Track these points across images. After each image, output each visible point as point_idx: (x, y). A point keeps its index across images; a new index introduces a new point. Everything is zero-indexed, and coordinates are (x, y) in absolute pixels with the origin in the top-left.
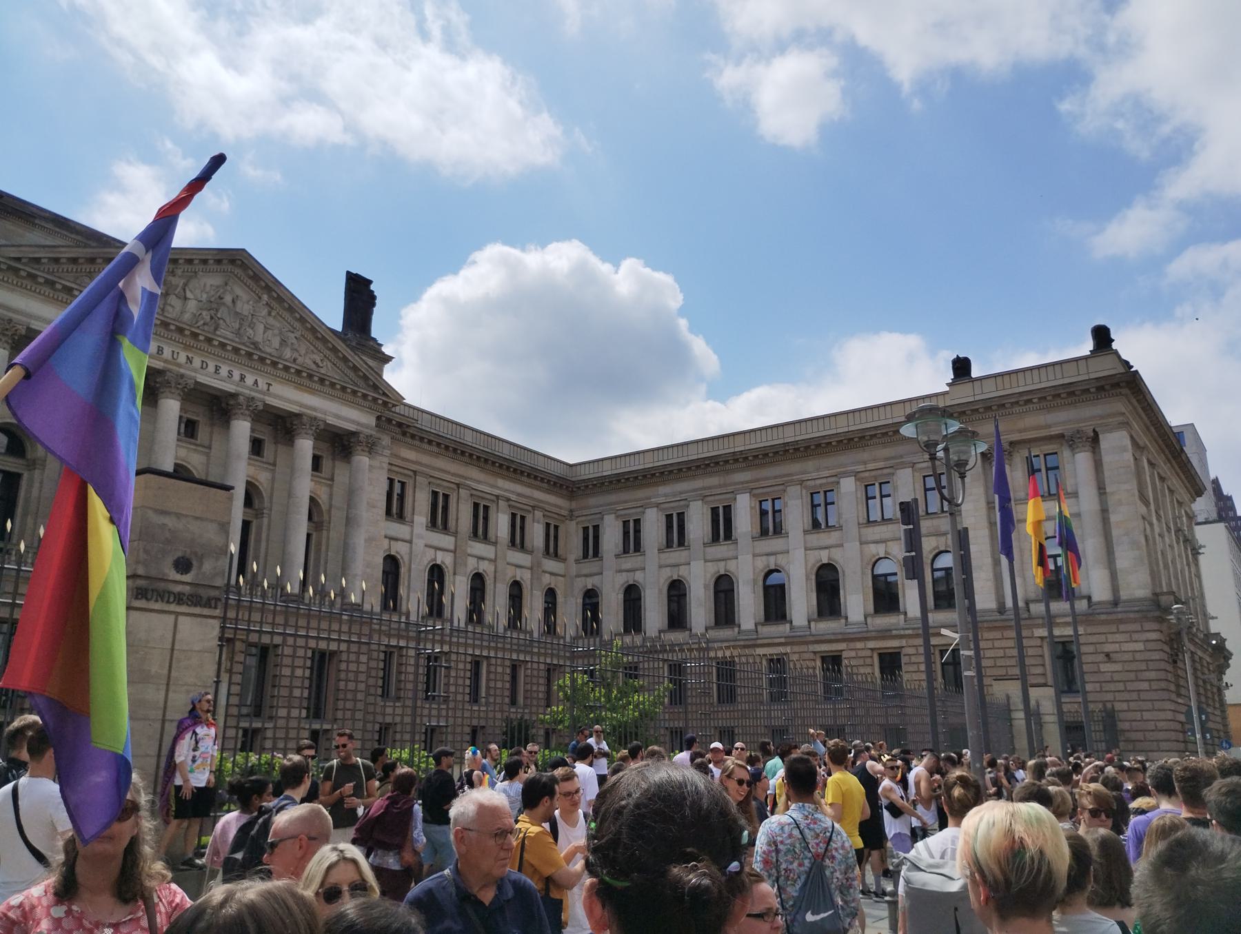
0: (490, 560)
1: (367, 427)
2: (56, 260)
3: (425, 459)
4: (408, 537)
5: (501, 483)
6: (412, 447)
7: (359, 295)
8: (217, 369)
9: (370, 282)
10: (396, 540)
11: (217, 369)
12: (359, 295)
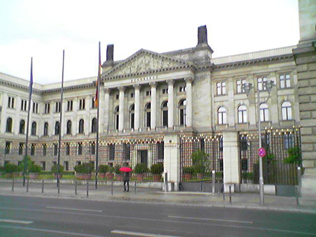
3: (230, 72)
4: (227, 99)
6: (225, 70)
7: (202, 32)
8: (144, 79)
9: (205, 26)
10: (222, 101)
11: (144, 79)
12: (202, 32)
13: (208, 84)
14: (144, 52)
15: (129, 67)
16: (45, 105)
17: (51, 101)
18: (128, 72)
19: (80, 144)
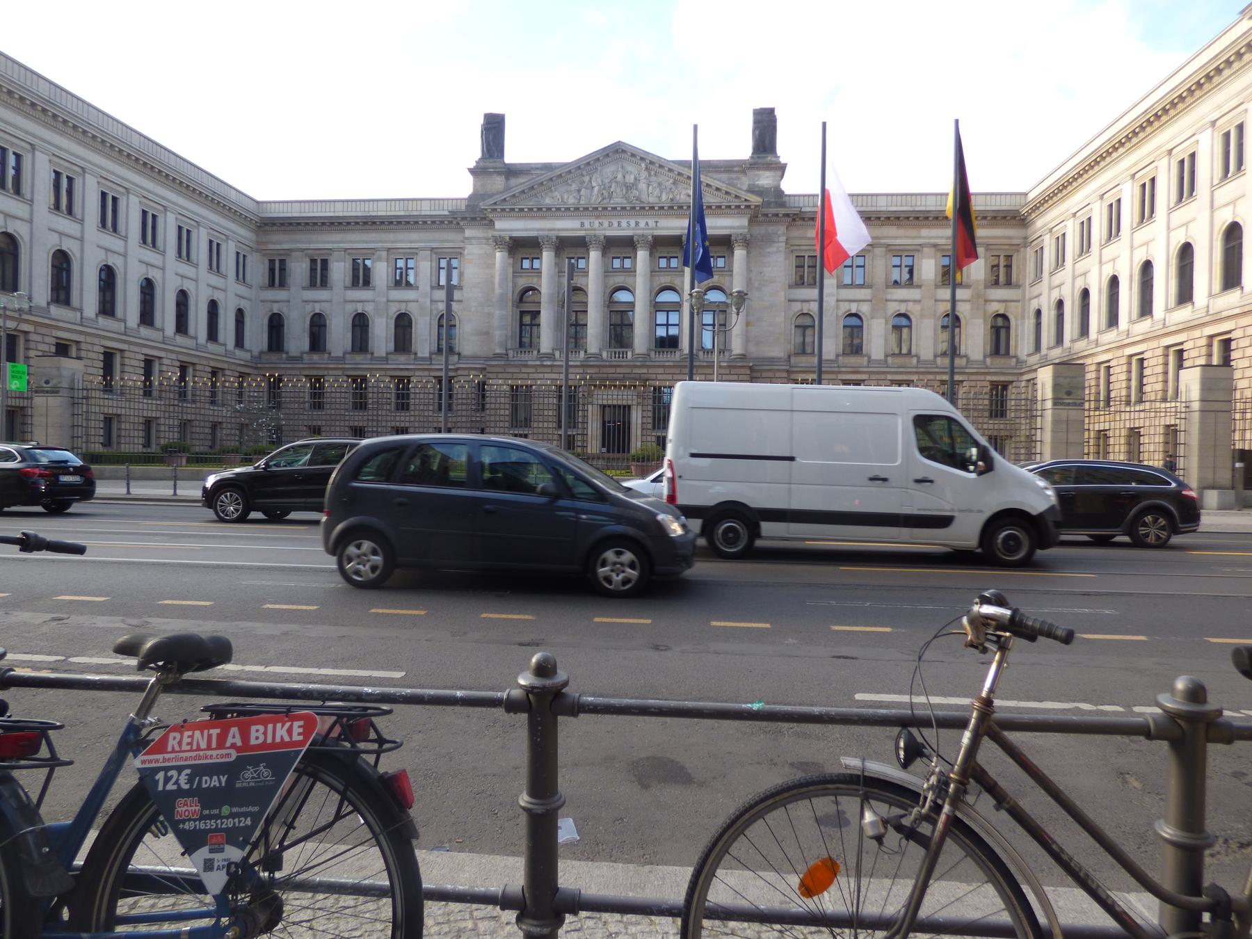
0: (915, 301)
1: (739, 227)
2: (514, 196)
5: (924, 232)
7: (765, 125)
8: (619, 224)
11: (619, 224)
12: (765, 125)
13: (780, 258)
14: (623, 151)
15: (574, 187)
16: (267, 262)
17: (290, 250)
18: (572, 201)
19: (402, 383)
